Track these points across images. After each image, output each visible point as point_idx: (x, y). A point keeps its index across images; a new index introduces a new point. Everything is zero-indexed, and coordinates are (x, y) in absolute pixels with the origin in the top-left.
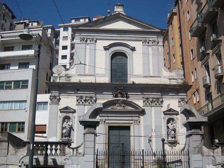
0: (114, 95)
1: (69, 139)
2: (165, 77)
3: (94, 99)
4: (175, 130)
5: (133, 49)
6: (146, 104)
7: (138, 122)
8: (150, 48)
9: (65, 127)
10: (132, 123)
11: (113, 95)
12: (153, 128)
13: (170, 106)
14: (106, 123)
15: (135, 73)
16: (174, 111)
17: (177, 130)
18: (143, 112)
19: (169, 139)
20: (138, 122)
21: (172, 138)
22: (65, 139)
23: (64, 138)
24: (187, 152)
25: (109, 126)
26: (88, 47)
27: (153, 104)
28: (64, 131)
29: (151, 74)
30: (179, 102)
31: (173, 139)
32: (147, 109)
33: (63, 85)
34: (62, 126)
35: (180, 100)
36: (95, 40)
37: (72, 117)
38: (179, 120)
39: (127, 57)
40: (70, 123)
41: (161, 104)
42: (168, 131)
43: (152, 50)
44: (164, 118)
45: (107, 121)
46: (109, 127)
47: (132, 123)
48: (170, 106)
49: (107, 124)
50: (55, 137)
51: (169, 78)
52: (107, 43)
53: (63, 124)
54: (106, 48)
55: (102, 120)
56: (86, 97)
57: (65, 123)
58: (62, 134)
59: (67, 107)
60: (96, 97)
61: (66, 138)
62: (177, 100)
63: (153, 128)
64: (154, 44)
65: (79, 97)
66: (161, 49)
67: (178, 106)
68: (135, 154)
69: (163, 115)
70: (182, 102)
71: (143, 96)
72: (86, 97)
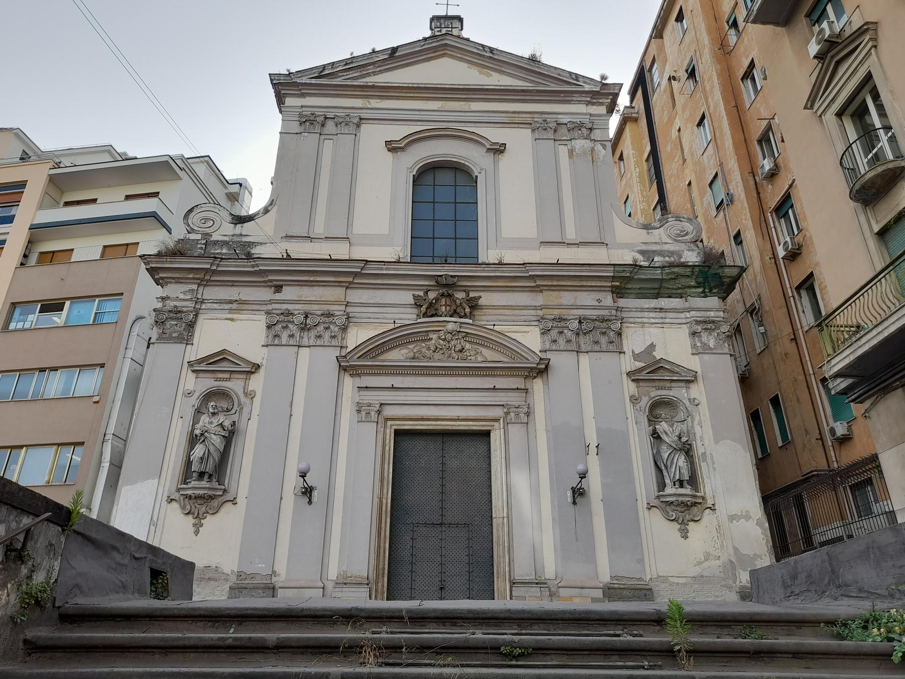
0: (423, 309)
1: (215, 485)
2: (627, 246)
4: (687, 449)
5: (498, 150)
6: (555, 341)
8: (563, 151)
9: (202, 435)
10: (497, 420)
12: (592, 439)
13: (654, 353)
14: (387, 419)
15: (508, 231)
17: (699, 449)
18: (542, 370)
19: (669, 490)
20: (522, 415)
21: (681, 486)
23: (194, 484)
26: (328, 145)
27: (585, 342)
28: (199, 451)
30: (694, 334)
31: (687, 490)
32: (556, 359)
34: (192, 431)
35: (699, 328)
36: (356, 120)
37: (241, 395)
38: (704, 408)
39: (473, 181)
41: (616, 340)
42: (659, 452)
43: (571, 152)
44: (634, 400)
45: (389, 412)
46: (398, 433)
47: (497, 420)
48: (654, 353)
49: (389, 423)
50: (156, 481)
51: (644, 248)
52: (398, 132)
53: (195, 421)
54: (393, 147)
55: (370, 405)
57: (204, 419)
58: (188, 463)
59: (223, 351)
60: (348, 314)
61: (204, 483)
62: (685, 331)
63: (592, 439)
65: (278, 315)
67: (690, 350)
69: (630, 388)
71: (540, 313)
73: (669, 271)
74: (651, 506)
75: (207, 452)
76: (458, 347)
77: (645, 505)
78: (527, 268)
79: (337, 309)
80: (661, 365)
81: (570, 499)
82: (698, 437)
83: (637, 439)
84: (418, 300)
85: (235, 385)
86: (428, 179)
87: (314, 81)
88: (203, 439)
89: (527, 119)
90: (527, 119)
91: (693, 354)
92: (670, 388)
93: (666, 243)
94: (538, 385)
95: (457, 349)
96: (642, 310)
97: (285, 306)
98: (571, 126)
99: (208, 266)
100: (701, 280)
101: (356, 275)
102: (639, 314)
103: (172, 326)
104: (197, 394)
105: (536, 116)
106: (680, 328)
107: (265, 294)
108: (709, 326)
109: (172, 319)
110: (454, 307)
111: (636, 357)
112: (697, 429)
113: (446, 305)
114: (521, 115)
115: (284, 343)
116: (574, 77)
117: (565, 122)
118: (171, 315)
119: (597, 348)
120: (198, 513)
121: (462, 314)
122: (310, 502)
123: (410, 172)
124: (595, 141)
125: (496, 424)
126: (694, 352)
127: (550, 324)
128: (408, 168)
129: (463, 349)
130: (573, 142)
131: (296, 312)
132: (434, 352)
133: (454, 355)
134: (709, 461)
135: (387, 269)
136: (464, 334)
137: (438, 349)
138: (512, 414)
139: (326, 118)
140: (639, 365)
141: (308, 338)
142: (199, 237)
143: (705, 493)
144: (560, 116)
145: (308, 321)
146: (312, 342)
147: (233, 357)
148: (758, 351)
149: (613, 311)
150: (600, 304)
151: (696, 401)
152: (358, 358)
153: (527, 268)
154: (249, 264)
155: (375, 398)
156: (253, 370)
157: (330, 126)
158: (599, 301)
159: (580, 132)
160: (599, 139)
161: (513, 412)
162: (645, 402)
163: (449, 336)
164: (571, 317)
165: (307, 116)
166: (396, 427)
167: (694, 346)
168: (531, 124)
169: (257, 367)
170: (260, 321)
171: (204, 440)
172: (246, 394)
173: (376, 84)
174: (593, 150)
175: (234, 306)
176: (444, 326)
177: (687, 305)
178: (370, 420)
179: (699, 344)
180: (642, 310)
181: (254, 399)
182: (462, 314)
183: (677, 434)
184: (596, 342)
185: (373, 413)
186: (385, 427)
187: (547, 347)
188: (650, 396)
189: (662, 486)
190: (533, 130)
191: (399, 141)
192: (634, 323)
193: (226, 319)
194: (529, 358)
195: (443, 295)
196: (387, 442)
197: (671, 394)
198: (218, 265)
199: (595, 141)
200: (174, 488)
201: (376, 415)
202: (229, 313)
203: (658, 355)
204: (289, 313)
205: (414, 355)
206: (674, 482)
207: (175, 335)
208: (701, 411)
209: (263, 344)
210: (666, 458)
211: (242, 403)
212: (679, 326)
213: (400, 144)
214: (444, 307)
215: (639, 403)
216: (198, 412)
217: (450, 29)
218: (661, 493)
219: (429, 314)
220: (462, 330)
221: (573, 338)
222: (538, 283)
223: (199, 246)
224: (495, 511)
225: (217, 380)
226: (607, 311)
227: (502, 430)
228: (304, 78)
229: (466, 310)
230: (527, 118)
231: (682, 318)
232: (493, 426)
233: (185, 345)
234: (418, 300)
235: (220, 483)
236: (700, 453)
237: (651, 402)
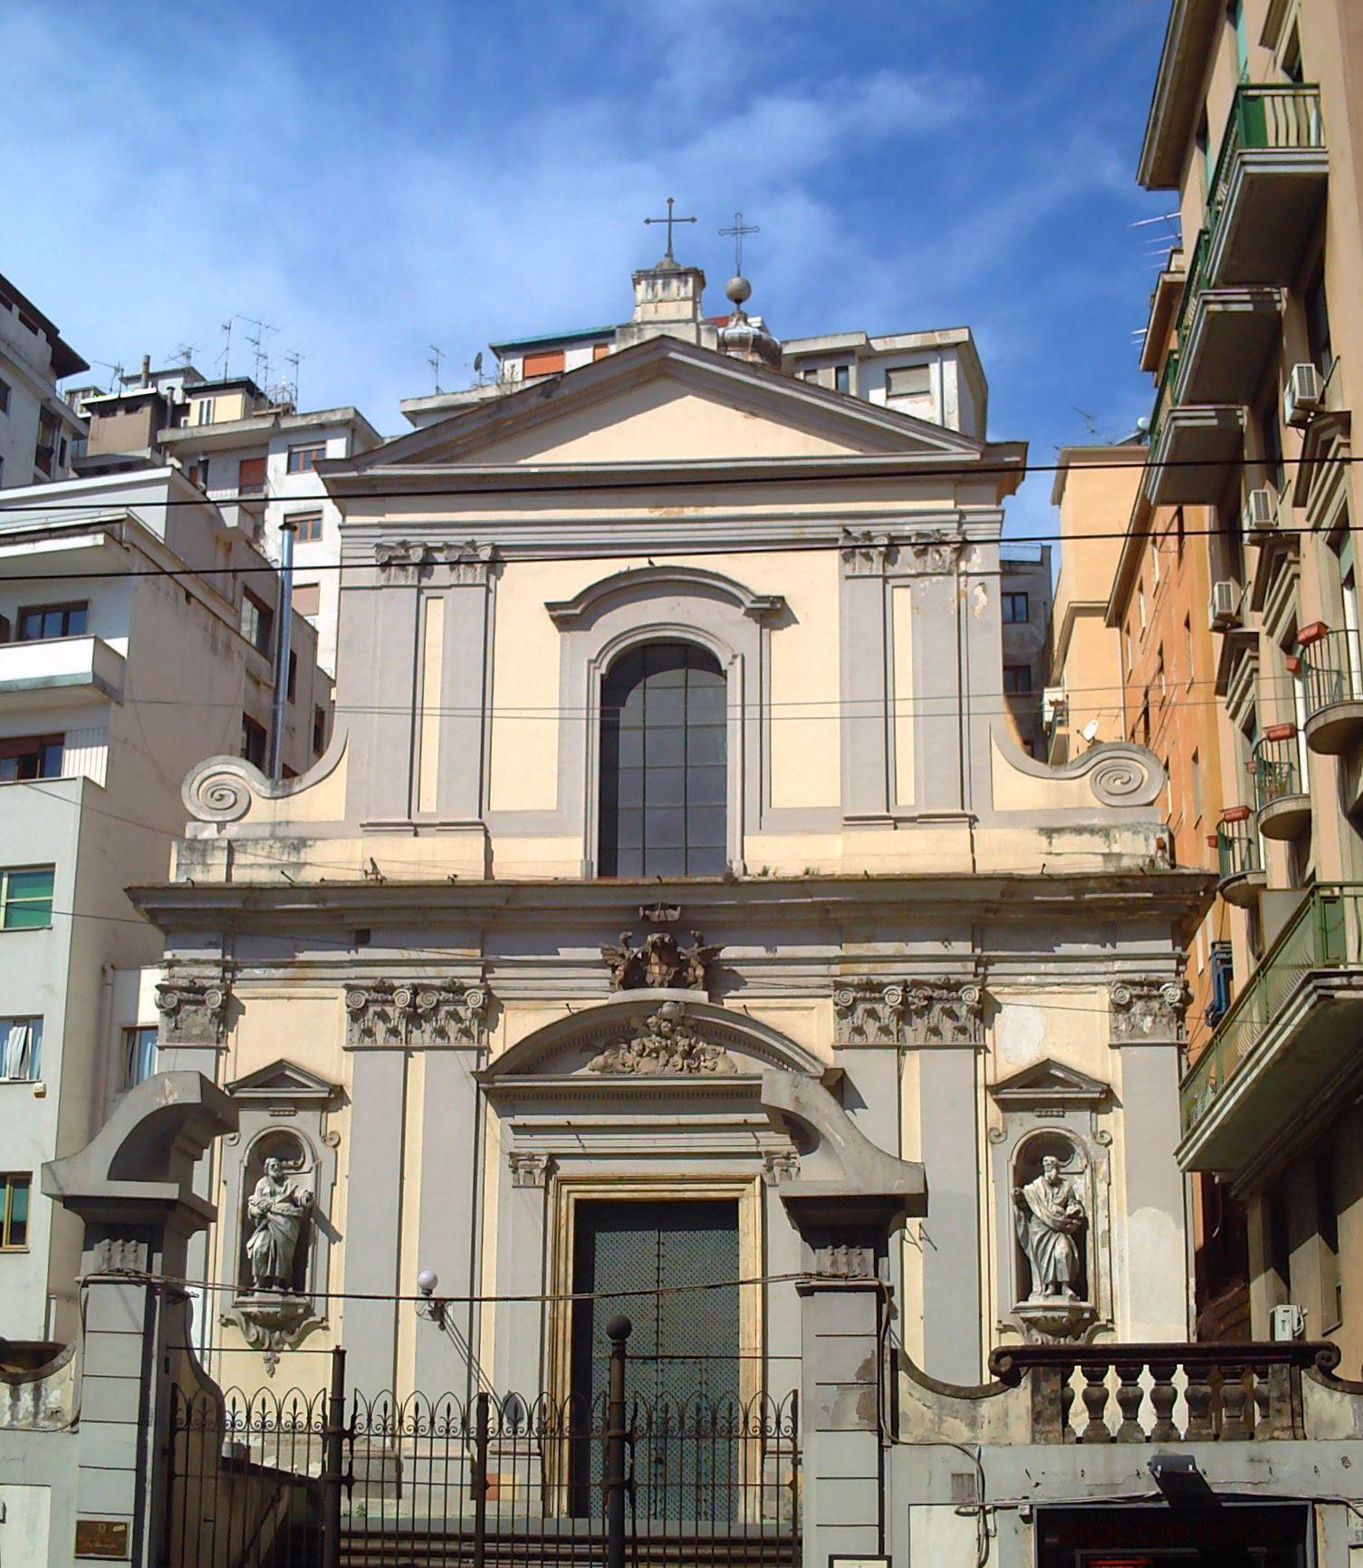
0: (620, 973)
2: (1012, 819)
3: (475, 999)
4: (1076, 1229)
9: (263, 1216)
10: (748, 1180)
11: (614, 968)
16: (1073, 1078)
19: (1034, 1300)
21: (1058, 1291)
22: (260, 1304)
25: (577, 1201)
27: (916, 1031)
28: (257, 1242)
29: (907, 798)
30: (1120, 1008)
40: (302, 1185)
45: (566, 1168)
47: (748, 1180)
49: (565, 1188)
52: (574, 578)
53: (249, 1190)
55: (532, 1158)
56: (416, 990)
57: (263, 1184)
58: (245, 1262)
66: (983, 598)
67: (1107, 1039)
68: (771, 1423)
70: (1138, 1007)
71: (836, 969)
72: (416, 990)
75: (272, 1244)
77: (995, 1325)
85: (303, 1123)
88: (264, 1222)
91: (1112, 1046)
109: (189, 1002)
115: (380, 1043)
117: (906, 534)
120: (270, 1343)
122: (442, 1327)
123: (595, 668)
126: (1115, 1042)
128: (590, 662)
137: (647, 1050)
145: (418, 1000)
146: (427, 1042)
155: (541, 1145)
157: (441, 575)
161: (778, 1164)
166: (578, 1196)
167: (1115, 1030)
170: (335, 998)
178: (531, 1183)
181: (339, 1148)
184: (935, 1031)
185: (537, 1172)
186: (558, 1197)
187: (845, 1041)
189: (1025, 1290)
190: (846, 558)
196: (563, 1221)
201: (543, 1176)
204: (385, 989)
205: (606, 1062)
209: (344, 1044)
212: (1093, 989)
218: (1022, 1304)
224: (743, 1338)
229: (697, 973)
232: (743, 1190)
235: (299, 1288)
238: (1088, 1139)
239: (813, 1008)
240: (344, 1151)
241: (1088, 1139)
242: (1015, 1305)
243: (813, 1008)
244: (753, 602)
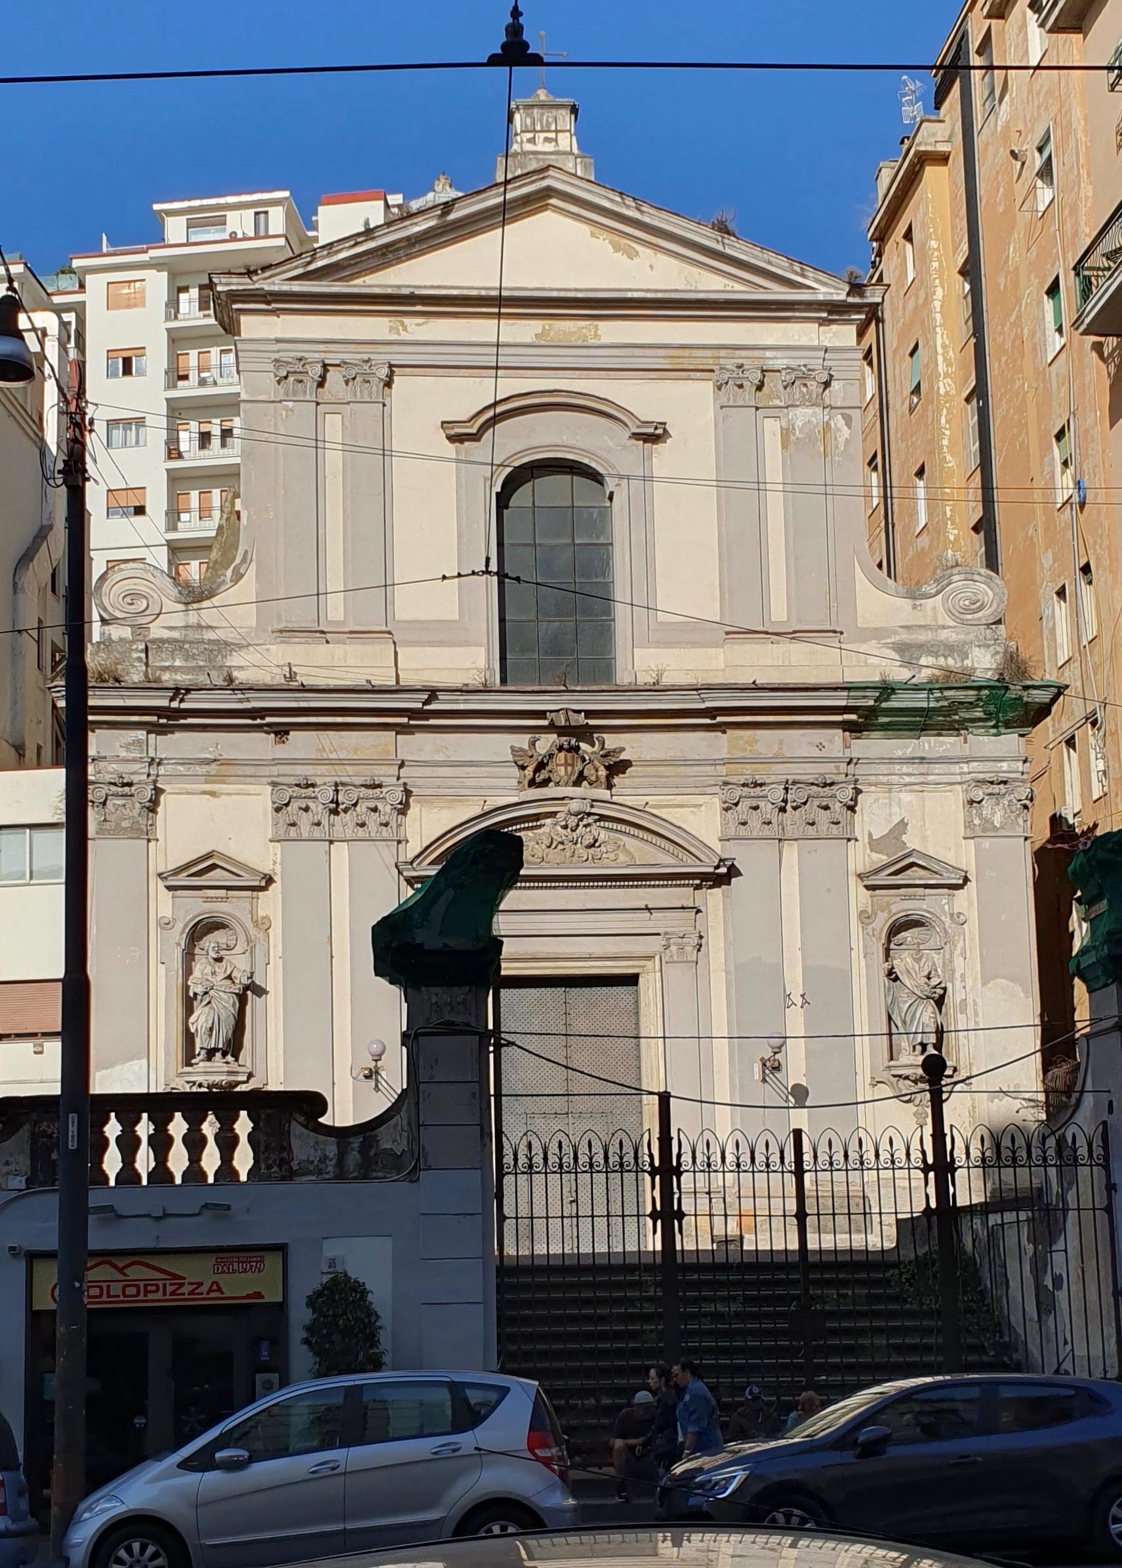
1: (234, 1067)
2: (877, 633)
5: (653, 436)
7: (689, 949)
8: (772, 428)
10: (650, 958)
11: (523, 768)
12: (795, 982)
13: (904, 838)
20: (689, 949)
24: (1097, 1142)
29: (779, 613)
33: (175, 704)
34: (186, 988)
36: (384, 372)
38: (972, 929)
40: (239, 964)
44: (865, 917)
47: (650, 958)
51: (905, 637)
53: (188, 972)
58: (189, 1038)
62: (957, 797)
63: (795, 982)
64: (798, 391)
66: (846, 432)
69: (859, 896)
70: (987, 804)
71: (722, 770)
73: (939, 695)
74: (878, 1082)
76: (589, 840)
77: (868, 1081)
78: (702, 696)
79: (386, 774)
80: (911, 860)
81: (757, 1076)
82: (957, 975)
83: (864, 981)
84: (521, 756)
86: (522, 497)
87: (297, 287)
89: (705, 361)
90: (705, 361)
91: (965, 838)
92: (923, 898)
93: (944, 627)
94: (714, 897)
95: (586, 843)
96: (892, 761)
97: (300, 770)
98: (788, 377)
99: (164, 703)
100: (992, 708)
101: (412, 713)
102: (884, 769)
103: (117, 807)
104: (179, 926)
105: (723, 353)
106: (950, 791)
107: (259, 744)
108: (996, 789)
110: (579, 766)
111: (875, 845)
112: (958, 962)
113: (566, 764)
114: (695, 353)
115: (305, 835)
116: (798, 270)
117: (776, 368)
118: (113, 788)
119: (811, 831)
121: (593, 778)
124: (832, 408)
125: (649, 964)
127: (738, 792)
129: (596, 841)
130: (792, 412)
131: (319, 781)
132: (549, 847)
133: (581, 851)
134: (970, 1011)
135: (466, 701)
136: (597, 817)
138: (673, 948)
139: (325, 367)
140: (882, 859)
141: (344, 824)
142: (127, 633)
143: (958, 1060)
144: (768, 354)
146: (349, 834)
147: (228, 863)
148: (1095, 798)
149: (841, 764)
150: (821, 754)
151: (962, 917)
152: (430, 864)
153: (702, 696)
154: (234, 697)
156: (263, 884)
158: (821, 746)
159: (804, 390)
160: (839, 404)
161: (675, 944)
162: (882, 923)
163: (573, 821)
164: (773, 779)
165: (288, 363)
167: (969, 824)
168: (712, 371)
169: (270, 880)
170: (259, 795)
171: (209, 1003)
172: (256, 924)
173: (417, 292)
174: (827, 427)
175: (213, 769)
176: (566, 805)
177: (966, 751)
179: (977, 821)
180: (892, 761)
181: (270, 931)
182: (593, 778)
183: (926, 973)
187: (732, 833)
188: (890, 911)
191: (469, 421)
192: (875, 785)
193: (204, 793)
194: (702, 857)
195: (560, 749)
197: (924, 907)
198: (182, 701)
199: (832, 408)
200: (173, 1073)
202: (207, 782)
203: (912, 841)
206: (914, 1047)
207: (125, 824)
208: (967, 932)
209: (270, 836)
210: (905, 1011)
211: (253, 938)
212: (949, 788)
213: (471, 427)
214: (563, 768)
215: (871, 923)
216: (189, 956)
217: (552, 135)
218: (892, 1063)
219: (538, 780)
220: (593, 811)
221: (774, 816)
222: (719, 719)
223: (135, 655)
225: (208, 900)
226: (833, 765)
227: (658, 974)
228: (276, 280)
230: (705, 359)
231: (955, 774)
232: (644, 966)
233: (145, 841)
234: (521, 756)
236: (958, 1000)
237: (891, 921)
238: (947, 920)
239: (701, 805)
240: (276, 933)
241: (947, 920)
242: (886, 1063)
243: (701, 805)
244: (638, 427)
